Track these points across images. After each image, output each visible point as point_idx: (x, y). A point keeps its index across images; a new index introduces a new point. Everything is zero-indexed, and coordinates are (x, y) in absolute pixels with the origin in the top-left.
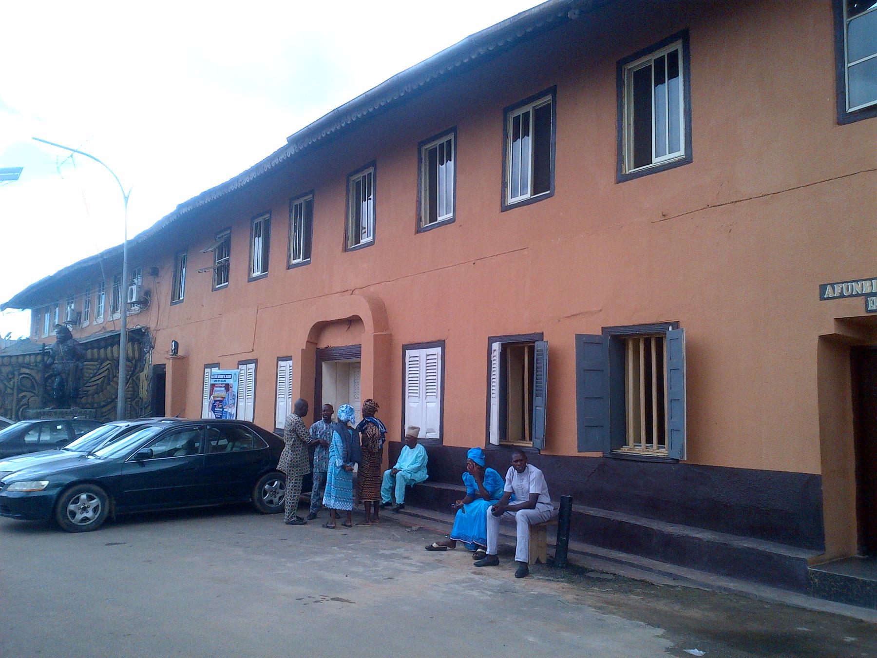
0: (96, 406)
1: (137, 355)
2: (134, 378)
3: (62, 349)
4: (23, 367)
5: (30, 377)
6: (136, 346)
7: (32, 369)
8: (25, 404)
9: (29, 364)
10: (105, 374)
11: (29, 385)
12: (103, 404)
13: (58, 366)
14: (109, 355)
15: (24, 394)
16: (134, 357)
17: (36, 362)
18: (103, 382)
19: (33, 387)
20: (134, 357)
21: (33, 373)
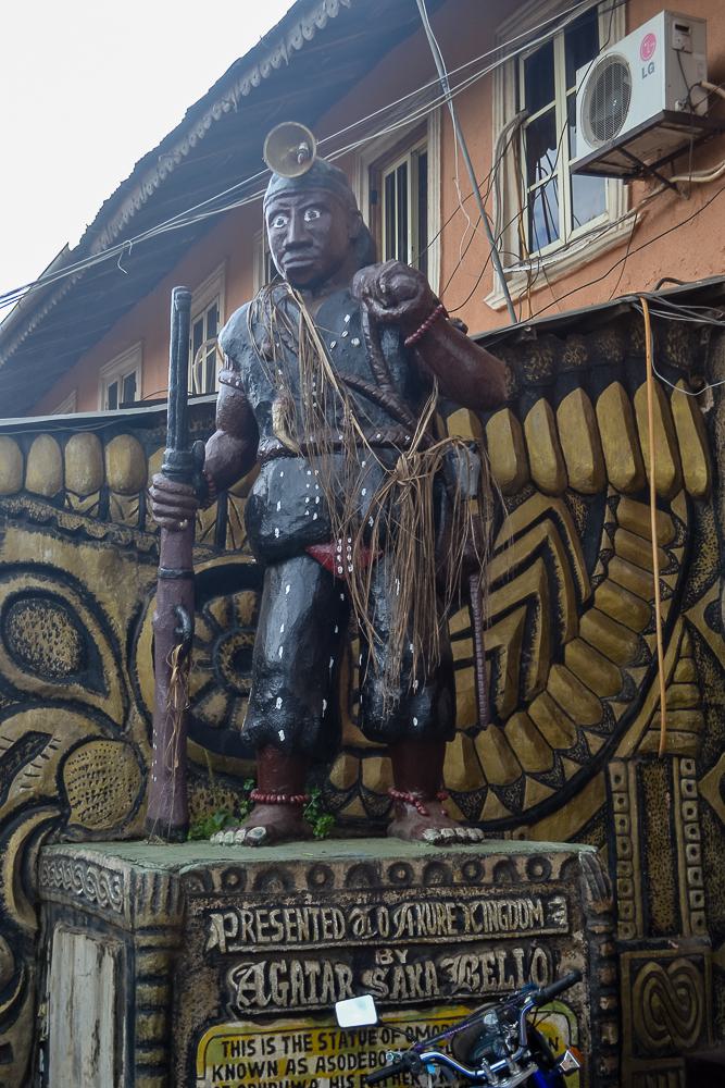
0: (493, 807)
1: (698, 474)
2: (697, 615)
3: (330, 338)
4: (23, 519)
5: (63, 594)
6: (681, 407)
7: (78, 536)
8: (40, 801)
9: (58, 497)
10: (530, 582)
11: (62, 652)
12: (535, 793)
13: (285, 488)
14: (543, 462)
15: (31, 719)
16: (678, 482)
17: (101, 486)
18: (523, 639)
19: (87, 662)
20: (678, 482)
21: (88, 561)
